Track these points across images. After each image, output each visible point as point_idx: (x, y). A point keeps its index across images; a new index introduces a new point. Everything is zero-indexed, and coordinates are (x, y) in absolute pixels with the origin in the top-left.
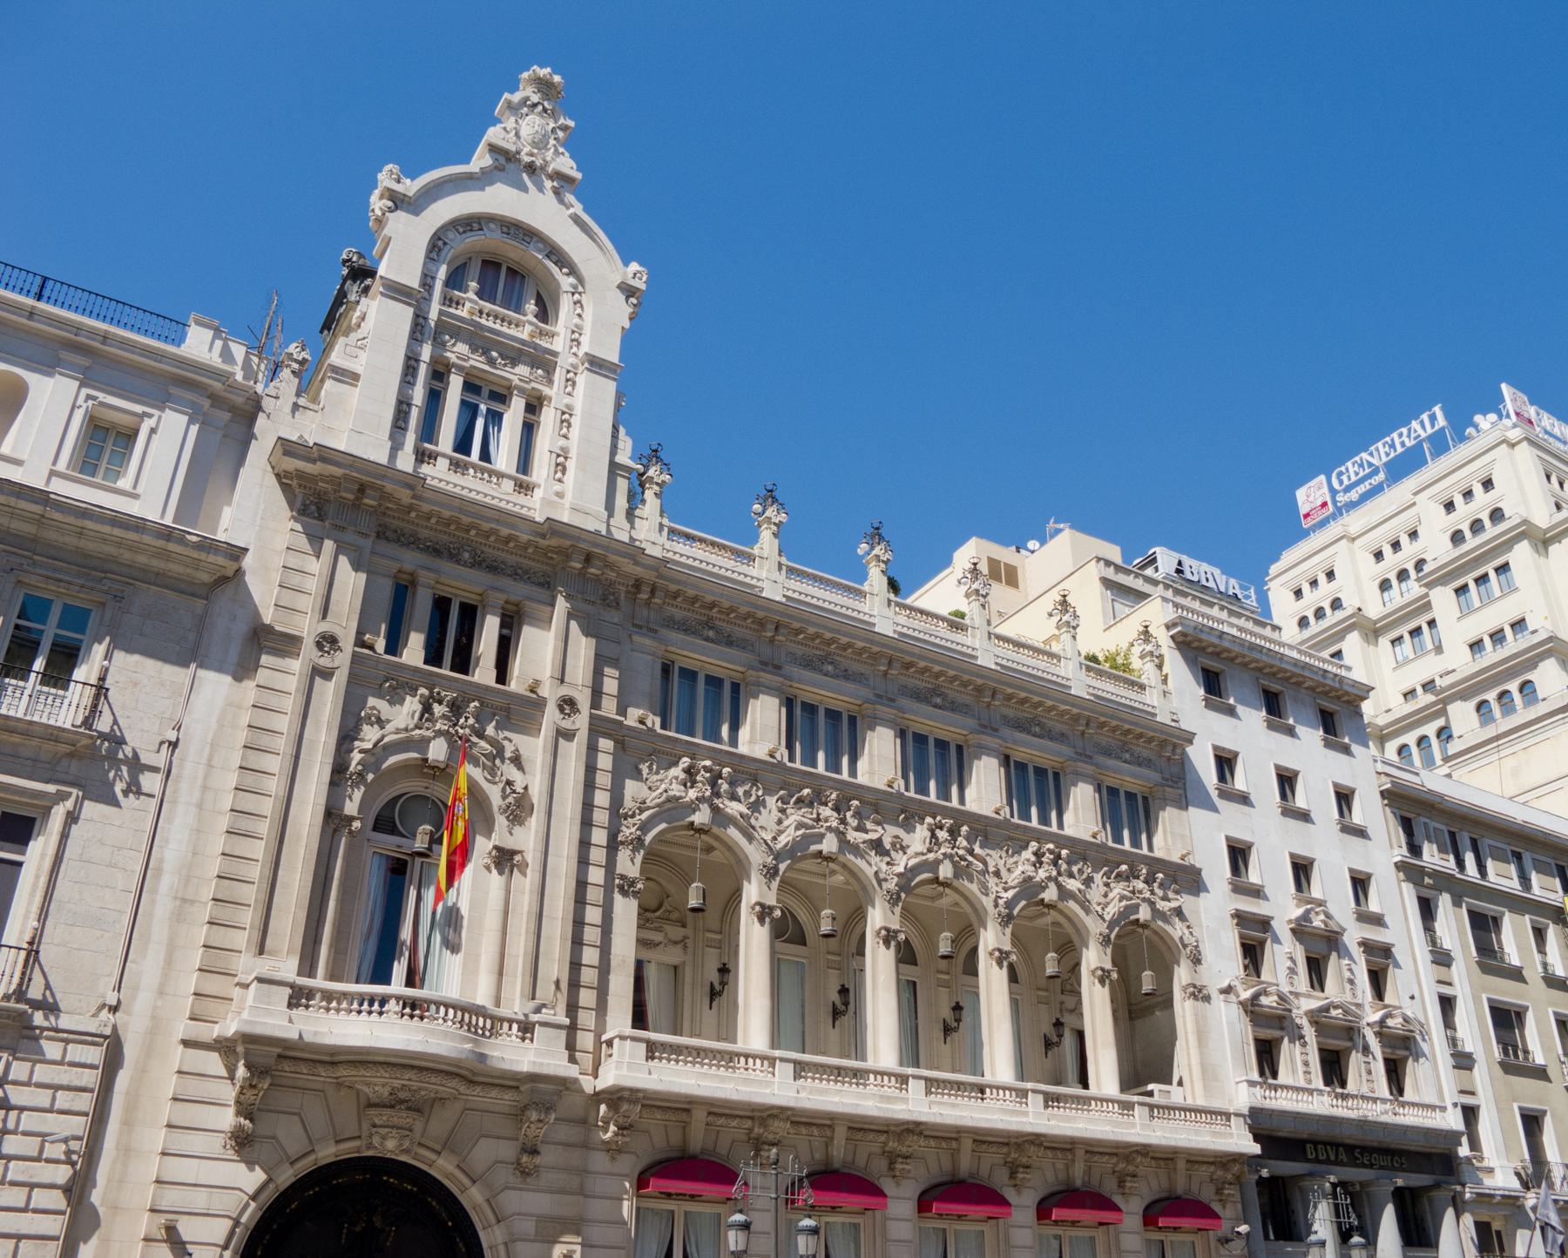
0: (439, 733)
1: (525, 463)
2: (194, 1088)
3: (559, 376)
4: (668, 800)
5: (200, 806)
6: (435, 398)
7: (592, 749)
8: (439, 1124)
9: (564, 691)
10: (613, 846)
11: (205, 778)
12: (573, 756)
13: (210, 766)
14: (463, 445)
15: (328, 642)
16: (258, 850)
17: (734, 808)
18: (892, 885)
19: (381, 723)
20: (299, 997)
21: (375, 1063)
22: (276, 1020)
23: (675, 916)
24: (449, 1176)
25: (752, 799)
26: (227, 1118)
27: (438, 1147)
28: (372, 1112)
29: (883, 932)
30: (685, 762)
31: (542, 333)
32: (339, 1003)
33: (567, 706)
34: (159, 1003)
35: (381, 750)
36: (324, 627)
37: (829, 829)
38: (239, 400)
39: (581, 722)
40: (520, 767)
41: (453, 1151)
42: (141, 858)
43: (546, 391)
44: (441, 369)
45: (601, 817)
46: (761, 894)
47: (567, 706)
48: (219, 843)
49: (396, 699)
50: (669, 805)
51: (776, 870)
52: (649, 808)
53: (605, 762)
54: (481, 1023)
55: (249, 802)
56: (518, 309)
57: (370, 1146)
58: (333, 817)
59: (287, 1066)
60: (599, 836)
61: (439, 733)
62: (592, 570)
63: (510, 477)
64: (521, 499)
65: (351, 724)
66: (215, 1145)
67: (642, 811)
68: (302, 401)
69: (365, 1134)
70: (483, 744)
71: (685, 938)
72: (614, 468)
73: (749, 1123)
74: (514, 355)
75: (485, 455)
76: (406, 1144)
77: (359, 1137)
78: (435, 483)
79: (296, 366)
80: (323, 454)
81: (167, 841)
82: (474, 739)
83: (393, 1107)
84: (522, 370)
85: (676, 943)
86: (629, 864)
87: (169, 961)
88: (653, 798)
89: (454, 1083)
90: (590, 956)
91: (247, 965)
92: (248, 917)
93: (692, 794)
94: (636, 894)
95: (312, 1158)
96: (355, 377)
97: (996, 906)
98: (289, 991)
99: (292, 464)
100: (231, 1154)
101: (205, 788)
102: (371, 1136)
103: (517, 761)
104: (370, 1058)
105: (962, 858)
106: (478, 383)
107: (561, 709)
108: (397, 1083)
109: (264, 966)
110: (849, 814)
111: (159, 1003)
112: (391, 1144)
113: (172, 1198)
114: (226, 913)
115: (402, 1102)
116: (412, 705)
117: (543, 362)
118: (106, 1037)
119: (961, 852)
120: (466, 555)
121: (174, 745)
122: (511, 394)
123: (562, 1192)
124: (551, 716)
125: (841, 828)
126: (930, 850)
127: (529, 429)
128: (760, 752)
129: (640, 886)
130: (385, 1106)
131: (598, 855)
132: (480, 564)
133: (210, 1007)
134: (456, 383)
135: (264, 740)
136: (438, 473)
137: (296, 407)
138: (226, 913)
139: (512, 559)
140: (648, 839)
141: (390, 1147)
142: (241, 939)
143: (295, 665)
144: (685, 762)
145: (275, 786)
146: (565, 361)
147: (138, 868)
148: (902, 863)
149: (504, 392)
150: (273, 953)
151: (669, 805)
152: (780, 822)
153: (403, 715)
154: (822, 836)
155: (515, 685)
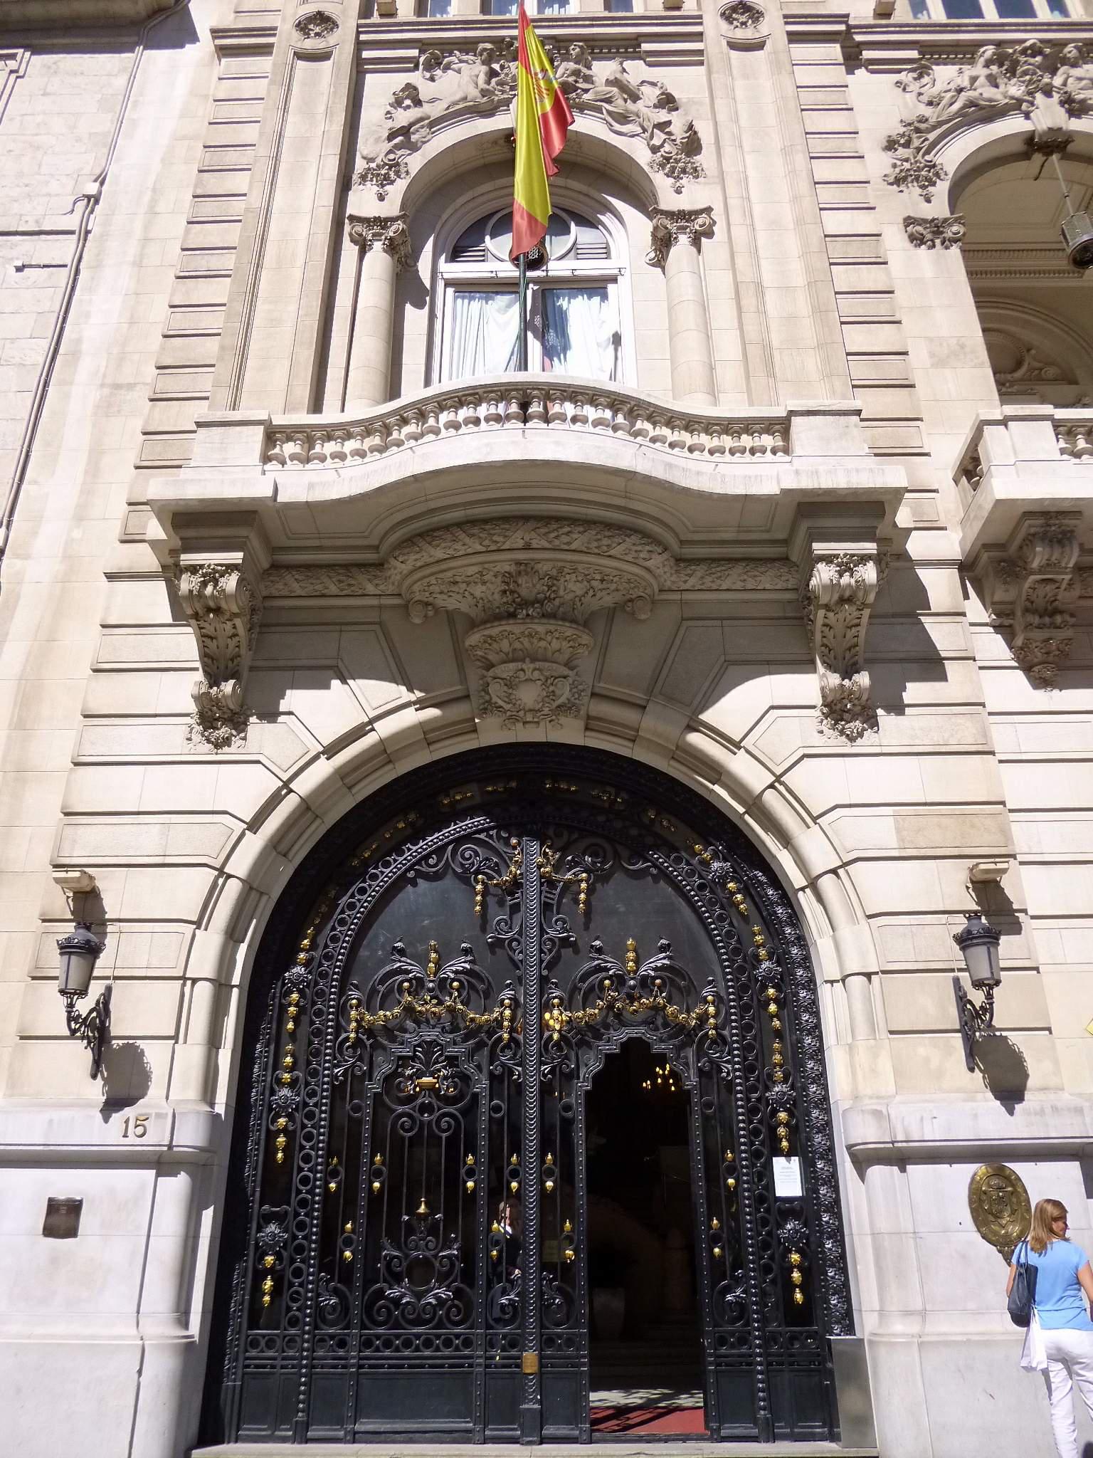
2: (129, 648)
5: (139, 263)
8: (632, 653)
11: (147, 227)
13: (152, 212)
21: (447, 527)
23: (1051, 372)
26: (183, 690)
27: (639, 696)
34: (77, 534)
41: (670, 699)
48: (165, 290)
59: (294, 584)
66: (178, 737)
69: (474, 684)
81: (88, 315)
83: (512, 615)
87: (93, 470)
98: (259, 431)
104: (436, 519)
111: (77, 534)
113: (88, 844)
130: (498, 618)
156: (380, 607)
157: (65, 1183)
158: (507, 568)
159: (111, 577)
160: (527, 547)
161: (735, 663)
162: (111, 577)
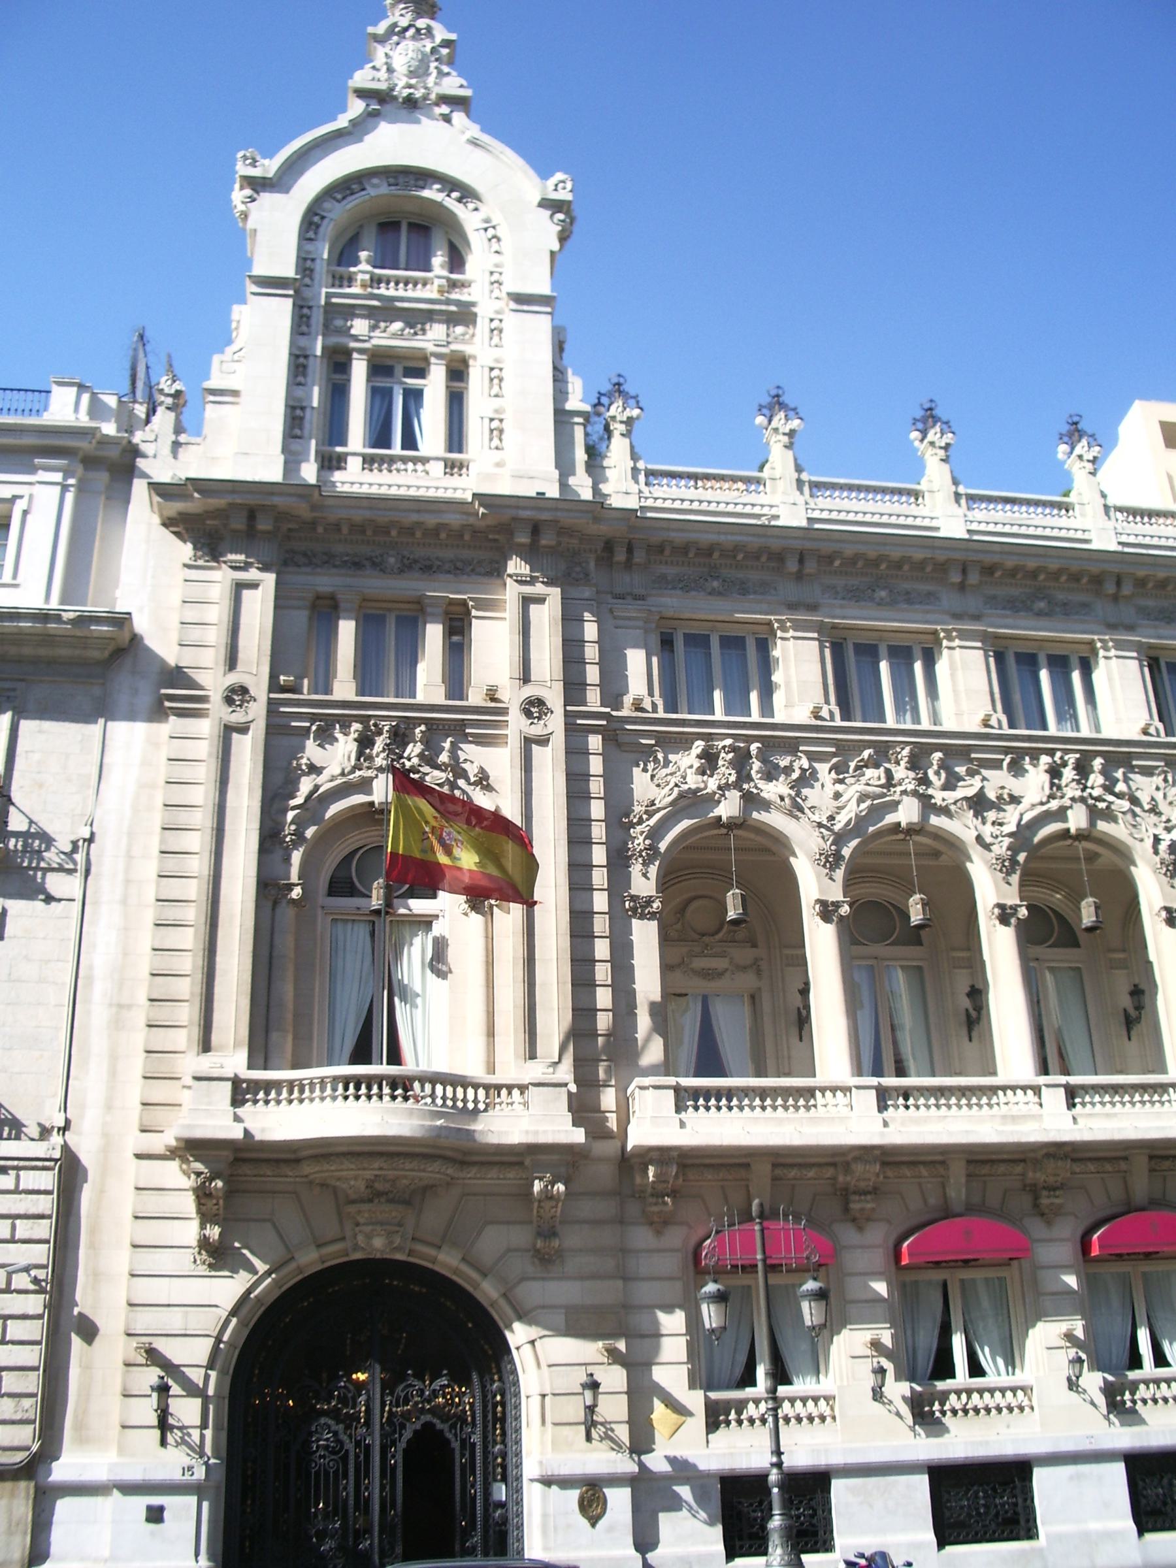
0: (381, 769)
1: (456, 438)
2: (153, 1204)
3: (482, 325)
4: (681, 796)
5: (124, 901)
6: (338, 393)
7: (575, 753)
8: (434, 1217)
9: (529, 691)
10: (619, 861)
12: (550, 765)
13: (129, 857)
14: (380, 436)
15: (237, 695)
16: (189, 939)
17: (773, 790)
18: (1001, 848)
19: (314, 769)
20: (242, 1092)
22: (219, 1122)
24: (456, 1271)
25: (795, 776)
26: (190, 1232)
28: (352, 1209)
29: (997, 911)
30: (698, 746)
31: (453, 285)
32: (267, 1094)
33: (534, 708)
35: (317, 802)
36: (233, 679)
37: (904, 792)
38: (114, 453)
39: (555, 724)
40: (488, 788)
42: (70, 967)
43: (467, 349)
44: (342, 359)
45: (598, 832)
46: (821, 891)
47: (534, 708)
48: (146, 938)
49: (325, 737)
50: (683, 802)
51: (838, 856)
52: (659, 810)
53: (596, 765)
54: (450, 1093)
55: (174, 889)
56: (428, 268)
57: (356, 1247)
58: (269, 888)
59: (246, 1169)
60: (599, 855)
61: (381, 769)
62: (543, 542)
63: (437, 459)
64: (455, 481)
65: (278, 778)
66: (185, 1261)
67: (650, 815)
68: (183, 438)
69: (348, 1234)
70: (436, 773)
71: (756, 960)
72: (562, 417)
73: (830, 1172)
74: (417, 319)
75: (410, 441)
76: (397, 1241)
77: (343, 1239)
78: (346, 488)
79: (169, 401)
80: (198, 484)
82: (426, 769)
83: (371, 1201)
84: (437, 331)
85: (744, 969)
86: (643, 883)
87: (113, 1073)
88: (664, 797)
89: (436, 1166)
90: (604, 997)
91: (193, 1063)
92: (187, 1014)
93: (712, 784)
94: (652, 916)
95: (292, 1266)
96: (235, 393)
97: (1156, 852)
99: (175, 507)
100: (203, 1270)
101: (128, 882)
102: (355, 1236)
103: (483, 781)
104: (331, 1150)
105: (1099, 799)
106: (389, 362)
107: (528, 714)
108: (369, 1174)
109: (206, 1064)
110: (931, 773)
112: (378, 1242)
113: (146, 1321)
114: (163, 1013)
115: (379, 1194)
116: (345, 747)
117: (464, 316)
118: (56, 1160)
119: (1096, 792)
120: (392, 560)
121: (90, 840)
122: (429, 364)
123: (594, 1277)
124: (516, 724)
125: (921, 789)
126: (1052, 796)
127: (456, 401)
128: (802, 716)
129: (656, 905)
130: (362, 1201)
131: (599, 877)
132: (410, 567)
133: (159, 1114)
134: (359, 370)
135: (183, 818)
136: (354, 479)
137: (176, 445)
138: (163, 1013)
139: (448, 554)
140: (663, 846)
141: (378, 1245)
142: (184, 1038)
143: (205, 727)
144: (698, 746)
145: (199, 865)
146: (484, 311)
147: (68, 979)
148: (1012, 818)
149: (421, 365)
150: (221, 1048)
151: (683, 802)
152: (837, 795)
153: (335, 757)
154: (898, 803)
155: (475, 697)
156: (295, 1182)
157: (156, 1500)
158: (368, 1177)
159: (139, 1156)
160: (381, 1169)
161: (492, 1223)
162: (139, 1156)
